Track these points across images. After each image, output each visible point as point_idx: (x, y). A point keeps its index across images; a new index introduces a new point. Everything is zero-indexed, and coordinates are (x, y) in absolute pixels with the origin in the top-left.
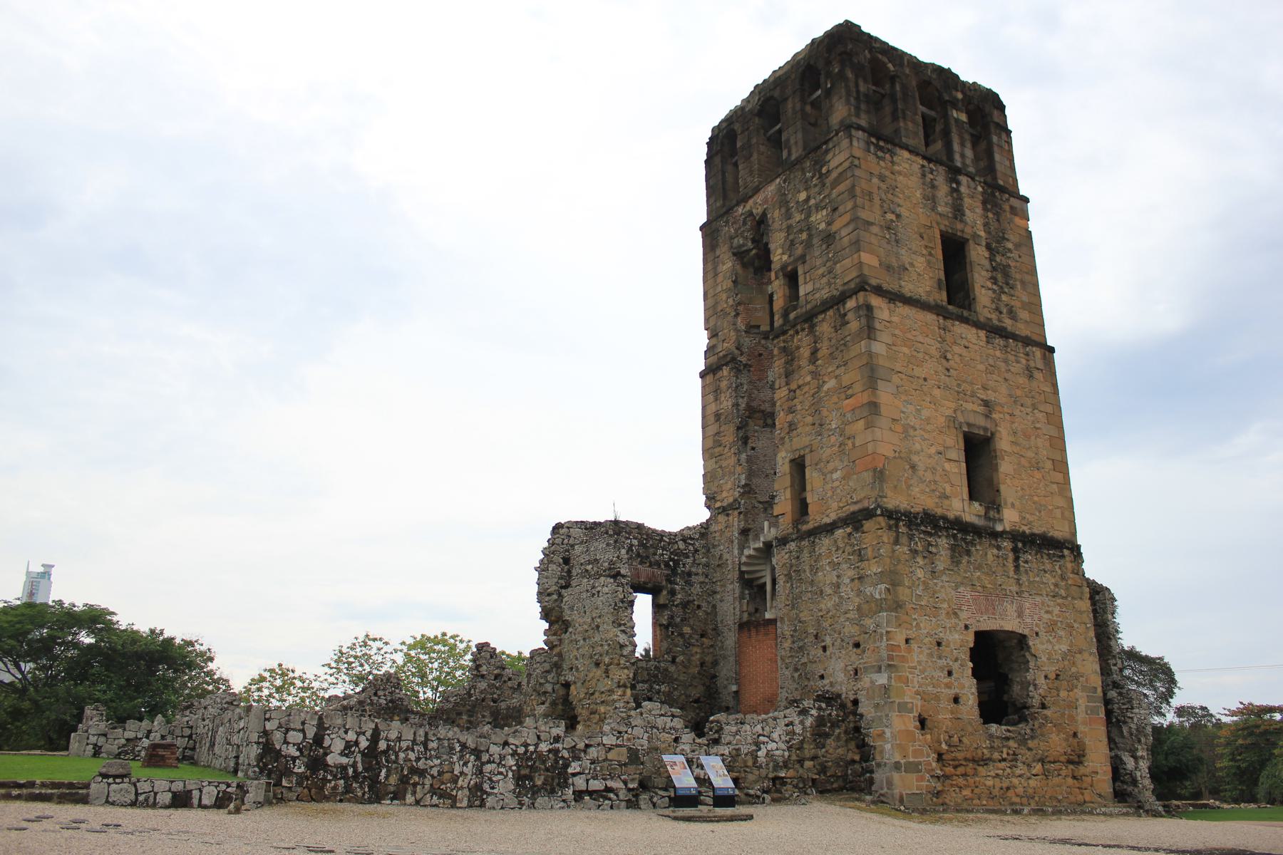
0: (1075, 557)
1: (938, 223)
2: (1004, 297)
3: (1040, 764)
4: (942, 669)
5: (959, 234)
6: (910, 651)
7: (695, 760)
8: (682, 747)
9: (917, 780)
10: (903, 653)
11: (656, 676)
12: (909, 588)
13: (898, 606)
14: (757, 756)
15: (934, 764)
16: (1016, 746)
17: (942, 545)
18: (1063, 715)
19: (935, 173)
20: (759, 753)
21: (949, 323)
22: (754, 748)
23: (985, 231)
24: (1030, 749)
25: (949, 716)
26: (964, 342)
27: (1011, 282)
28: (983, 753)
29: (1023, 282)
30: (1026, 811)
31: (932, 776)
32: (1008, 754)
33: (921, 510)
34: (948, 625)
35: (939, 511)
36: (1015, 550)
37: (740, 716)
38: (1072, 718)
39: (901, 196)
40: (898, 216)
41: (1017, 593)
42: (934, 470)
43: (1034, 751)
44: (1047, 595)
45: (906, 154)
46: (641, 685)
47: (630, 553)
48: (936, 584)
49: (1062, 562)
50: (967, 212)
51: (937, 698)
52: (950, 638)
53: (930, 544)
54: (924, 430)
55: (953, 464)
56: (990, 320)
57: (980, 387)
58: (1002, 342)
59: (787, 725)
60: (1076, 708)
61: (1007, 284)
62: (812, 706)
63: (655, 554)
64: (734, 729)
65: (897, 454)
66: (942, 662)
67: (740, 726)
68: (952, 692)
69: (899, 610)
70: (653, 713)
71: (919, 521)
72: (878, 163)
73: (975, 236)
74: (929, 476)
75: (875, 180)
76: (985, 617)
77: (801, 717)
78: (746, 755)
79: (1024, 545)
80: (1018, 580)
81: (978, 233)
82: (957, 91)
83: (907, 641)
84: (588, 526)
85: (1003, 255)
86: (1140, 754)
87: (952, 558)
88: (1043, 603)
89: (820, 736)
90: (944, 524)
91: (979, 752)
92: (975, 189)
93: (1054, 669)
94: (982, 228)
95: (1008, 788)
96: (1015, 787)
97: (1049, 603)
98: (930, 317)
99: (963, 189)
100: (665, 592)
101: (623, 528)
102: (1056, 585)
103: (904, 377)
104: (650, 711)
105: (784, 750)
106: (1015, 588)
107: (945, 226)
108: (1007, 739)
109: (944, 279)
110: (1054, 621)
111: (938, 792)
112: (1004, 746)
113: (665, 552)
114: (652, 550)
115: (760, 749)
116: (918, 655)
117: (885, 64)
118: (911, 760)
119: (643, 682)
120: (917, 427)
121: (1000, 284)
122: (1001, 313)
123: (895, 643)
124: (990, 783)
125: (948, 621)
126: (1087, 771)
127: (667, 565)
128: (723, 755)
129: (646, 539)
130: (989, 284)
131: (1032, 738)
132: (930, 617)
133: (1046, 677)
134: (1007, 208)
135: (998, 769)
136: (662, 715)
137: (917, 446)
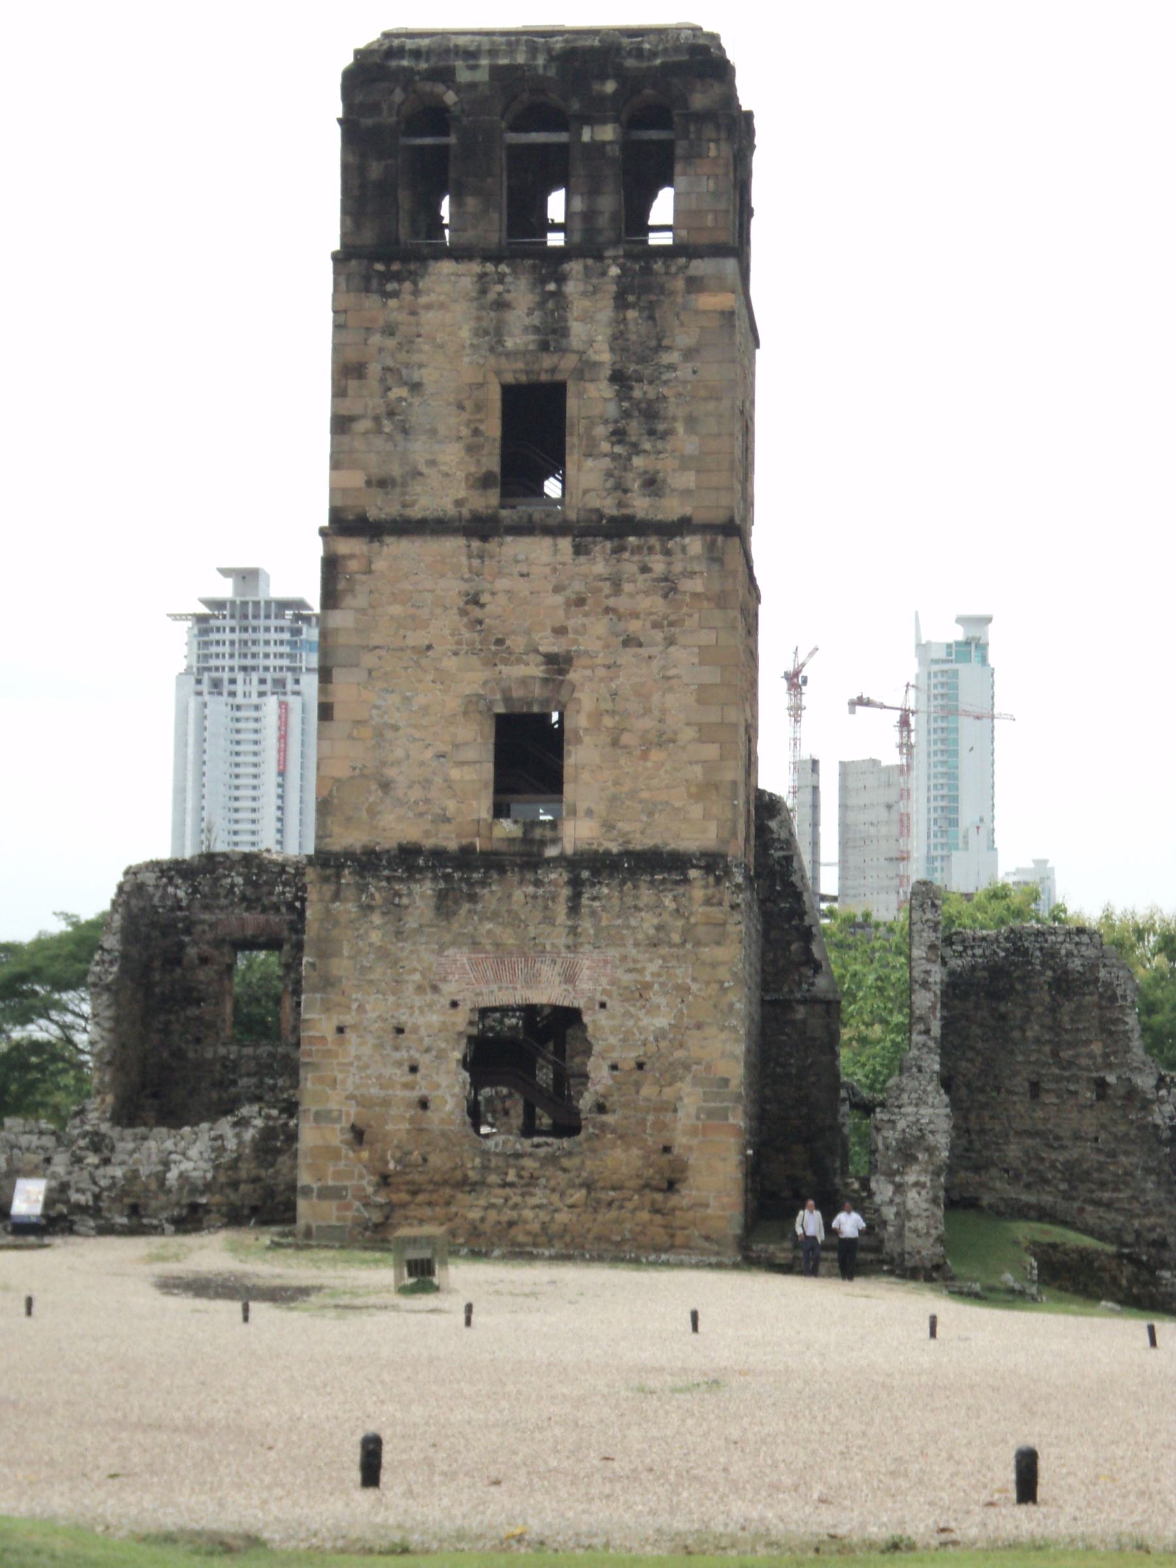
0: (718, 880)
1: (498, 373)
2: (638, 462)
3: (584, 1192)
4: (399, 1064)
5: (544, 377)
6: (342, 1043)
7: (72, 1184)
8: (52, 1168)
9: (339, 1208)
10: (330, 1046)
11: (270, 1066)
12: (350, 958)
13: (328, 983)
14: (164, 1179)
15: (370, 1190)
16: (537, 1165)
17: (423, 892)
18: (643, 1122)
19: (509, 279)
20: (169, 1175)
21: (492, 546)
22: (160, 1168)
23: (612, 350)
24: (565, 1170)
25: (408, 1126)
26: (517, 569)
27: (661, 427)
28: (466, 1176)
29: (691, 421)
30: (497, 1253)
31: (366, 1205)
32: (520, 1177)
33: (395, 845)
34: (417, 1004)
35: (428, 843)
36: (576, 884)
37: (141, 1130)
38: (661, 1126)
39: (426, 348)
40: (416, 387)
41: (568, 947)
42: (426, 783)
43: (572, 1174)
44: (637, 944)
45: (446, 267)
46: (245, 1080)
47: (230, 897)
48: (402, 949)
49: (681, 890)
50: (578, 330)
51: (386, 1102)
52: (421, 1021)
53: (398, 894)
54: (415, 727)
55: (466, 768)
56: (597, 511)
57: (549, 632)
58: (609, 545)
59: (215, 1139)
60: (675, 1110)
61: (652, 433)
62: (254, 1114)
63: (271, 893)
64: (131, 1146)
65: (357, 771)
66: (403, 1054)
67: (139, 1142)
68: (415, 1094)
69: (329, 989)
70: (15, 1130)
71: (384, 862)
72: (385, 304)
73: (585, 370)
74: (416, 794)
75: (376, 339)
76: (494, 987)
77: (237, 1130)
78: (148, 1177)
79: (596, 872)
80: (576, 928)
81: (597, 358)
82: (603, 77)
83: (341, 1030)
84: (165, 867)
85: (651, 382)
86: (911, 1178)
87: (438, 908)
88: (624, 958)
89: (266, 1151)
90: (426, 861)
91: (458, 1175)
92: (604, 273)
93: (633, 1055)
94: (606, 347)
95: (511, 1224)
96: (525, 1222)
97: (640, 957)
98: (453, 545)
99: (570, 288)
100: (286, 947)
101: (221, 863)
102: (659, 928)
103: (382, 653)
104: (10, 1129)
105: (205, 1171)
106: (562, 940)
107: (515, 371)
108: (518, 1156)
109: (497, 469)
110: (647, 983)
111: (377, 1226)
112: (508, 1166)
113: (288, 889)
114: (265, 889)
115: (169, 1170)
116: (354, 1045)
117: (439, 99)
118: (331, 1183)
119: (249, 1075)
120: (401, 724)
121: (634, 439)
122: (626, 491)
123: (317, 1034)
124: (475, 1214)
125: (417, 998)
126: (685, 1202)
127: (290, 907)
128: (113, 1178)
129: (256, 875)
130: (605, 447)
131: (569, 1154)
132: (384, 994)
133: (614, 1067)
134: (680, 284)
135: (497, 1196)
136: (25, 1133)
137: (399, 753)
